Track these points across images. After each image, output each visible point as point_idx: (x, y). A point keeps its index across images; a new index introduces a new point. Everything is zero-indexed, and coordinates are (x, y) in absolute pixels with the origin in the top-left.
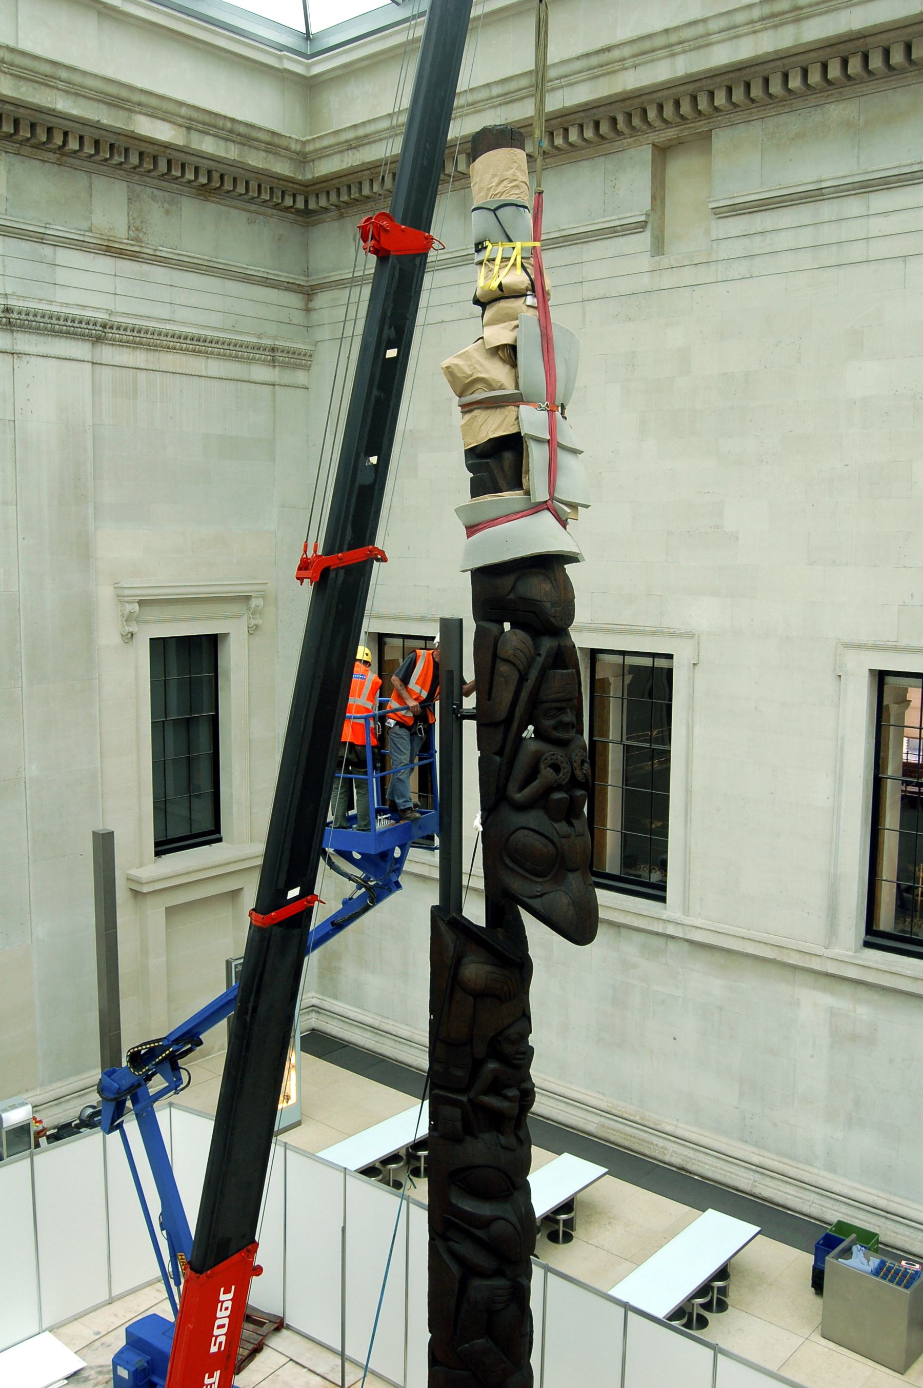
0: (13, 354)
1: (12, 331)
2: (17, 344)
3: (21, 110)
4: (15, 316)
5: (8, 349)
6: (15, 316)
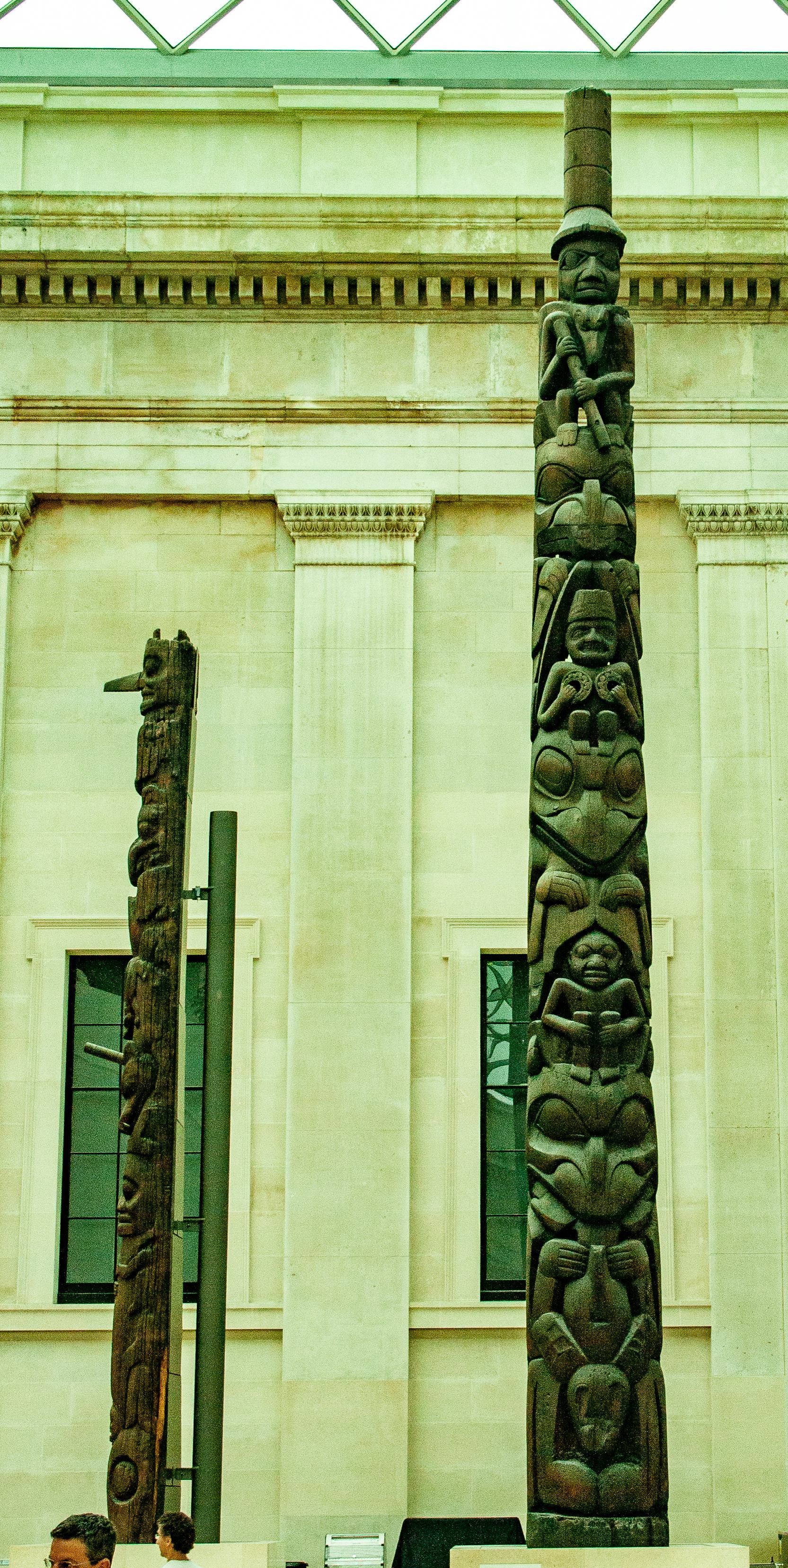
0: (765, 565)
1: (763, 537)
2: (770, 551)
3: (756, 269)
4: (762, 515)
5: (759, 559)
6: (762, 515)
